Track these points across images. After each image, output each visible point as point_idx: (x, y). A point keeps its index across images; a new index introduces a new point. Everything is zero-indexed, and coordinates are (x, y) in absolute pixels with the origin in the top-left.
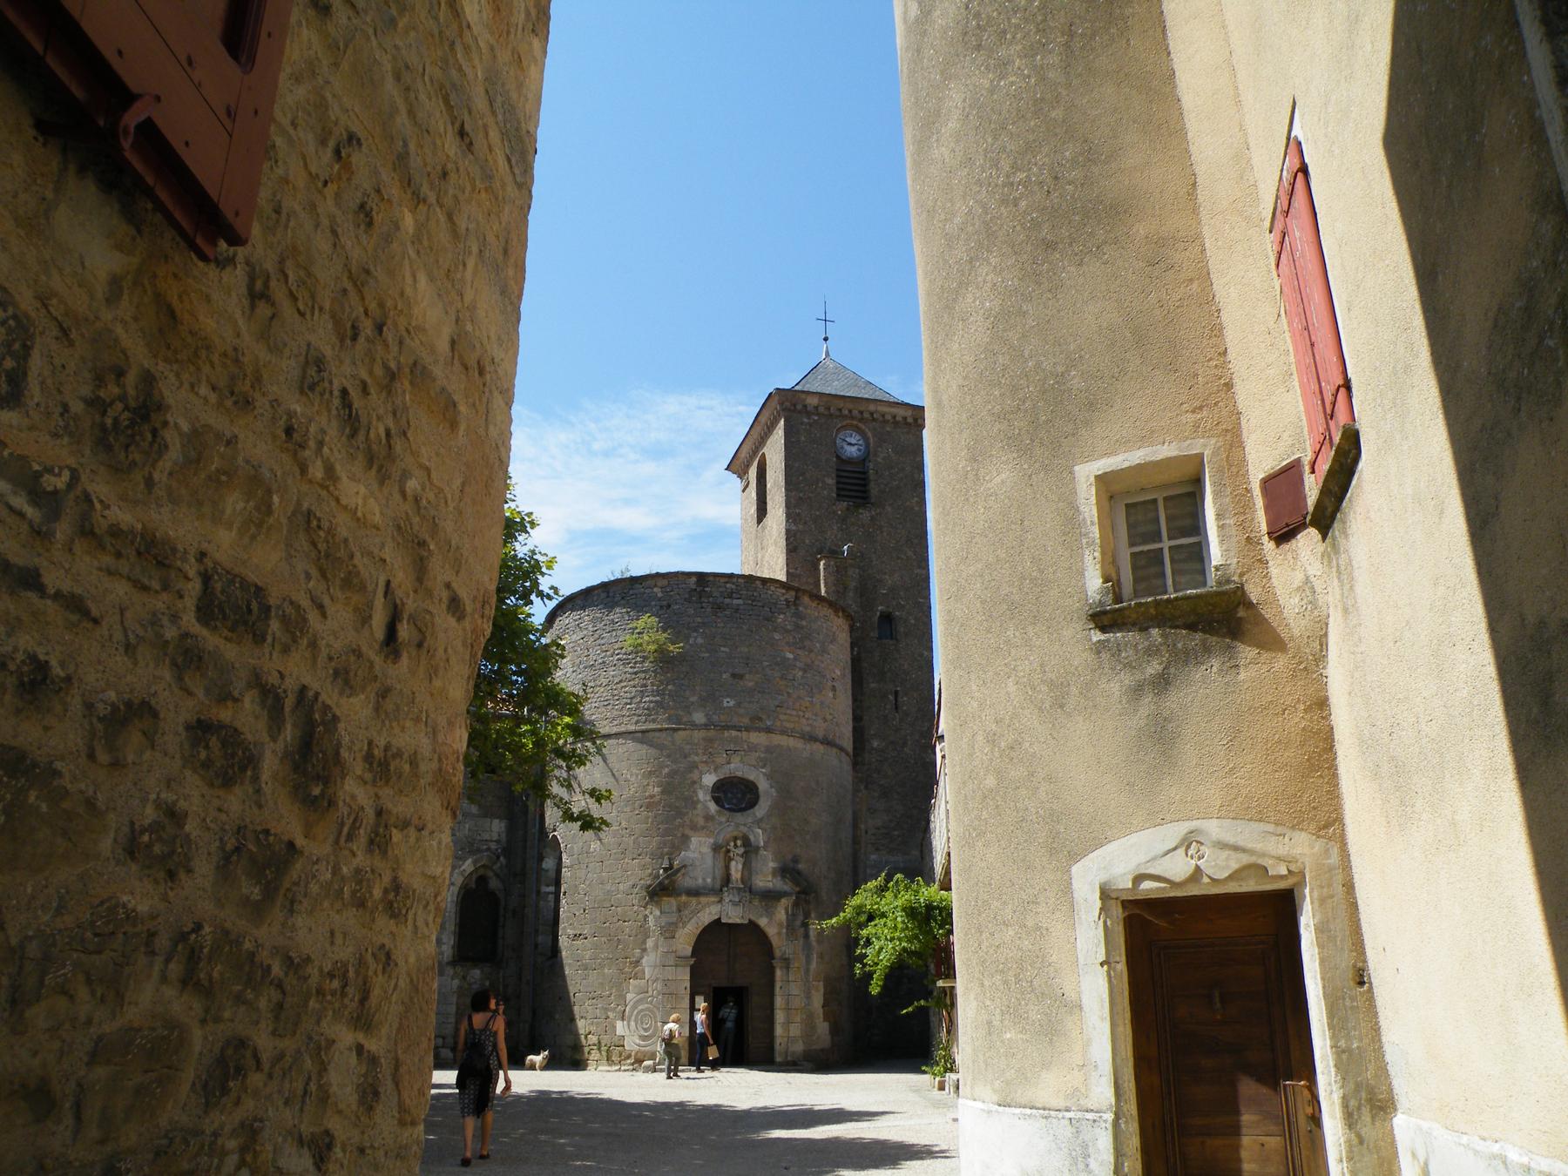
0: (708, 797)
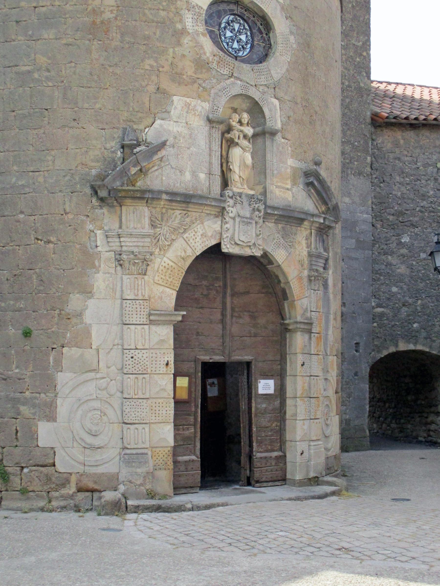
0: (201, 28)
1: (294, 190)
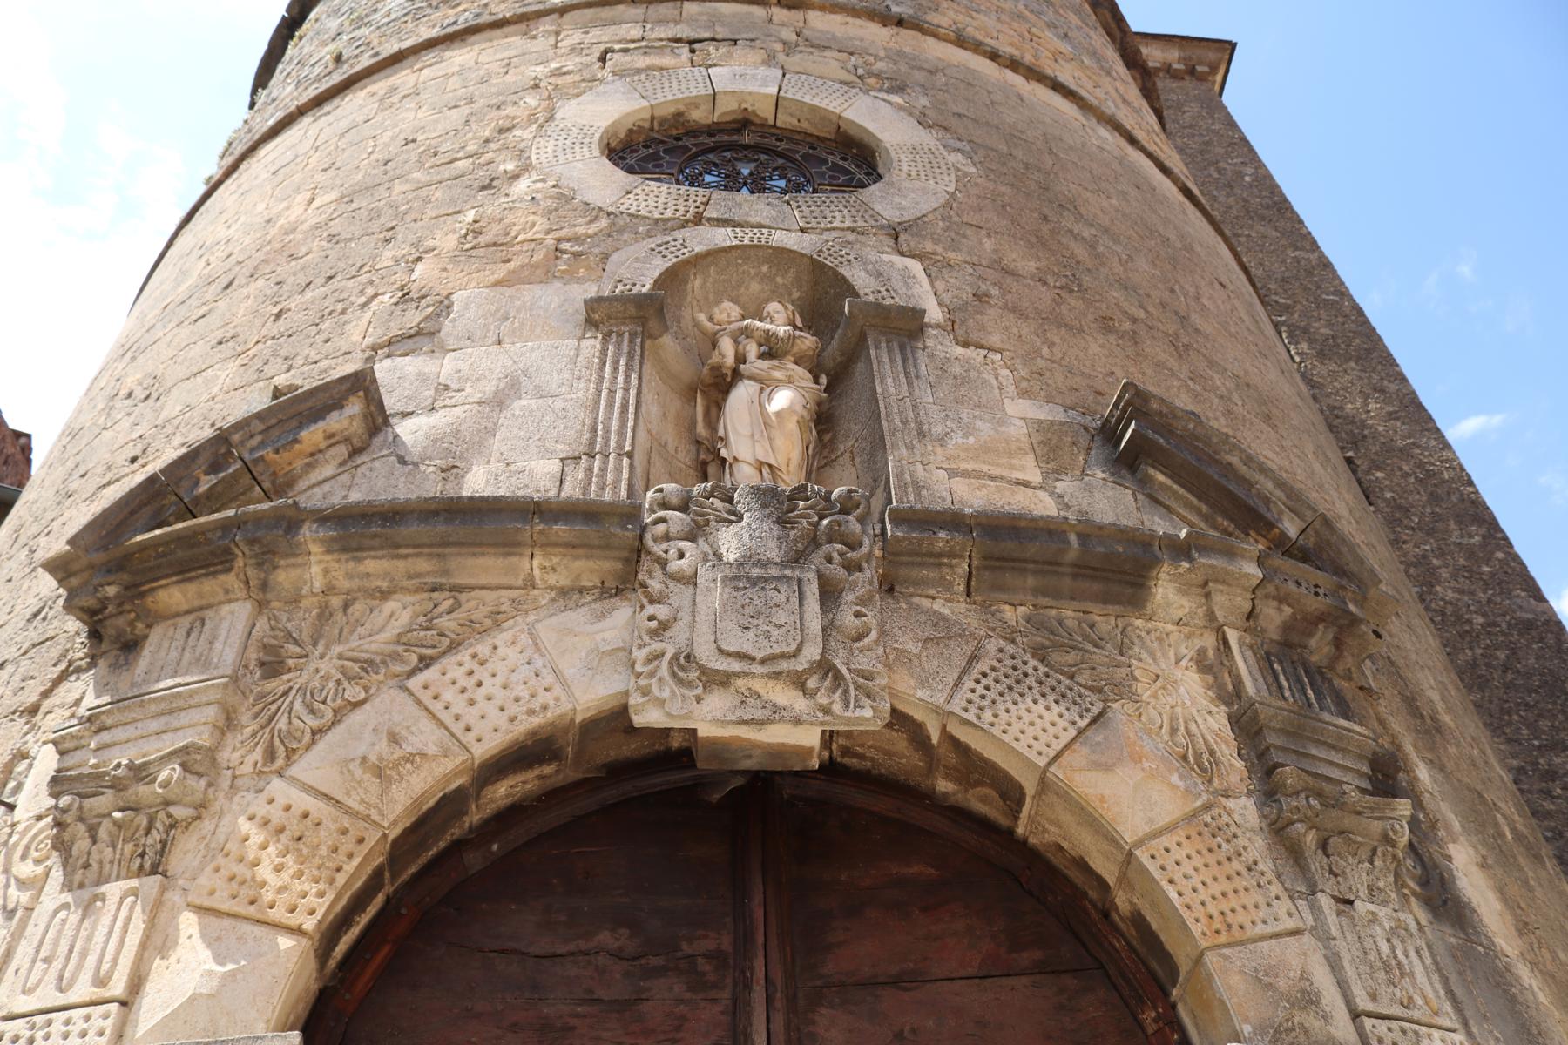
1: (1060, 486)
